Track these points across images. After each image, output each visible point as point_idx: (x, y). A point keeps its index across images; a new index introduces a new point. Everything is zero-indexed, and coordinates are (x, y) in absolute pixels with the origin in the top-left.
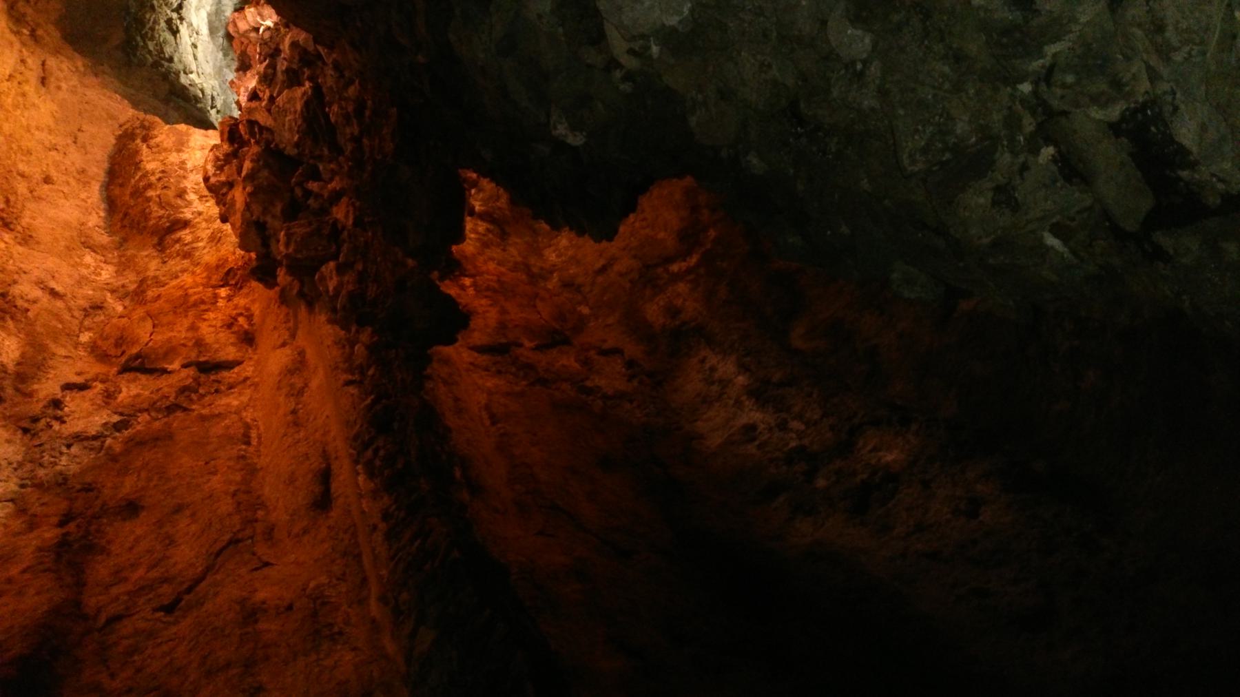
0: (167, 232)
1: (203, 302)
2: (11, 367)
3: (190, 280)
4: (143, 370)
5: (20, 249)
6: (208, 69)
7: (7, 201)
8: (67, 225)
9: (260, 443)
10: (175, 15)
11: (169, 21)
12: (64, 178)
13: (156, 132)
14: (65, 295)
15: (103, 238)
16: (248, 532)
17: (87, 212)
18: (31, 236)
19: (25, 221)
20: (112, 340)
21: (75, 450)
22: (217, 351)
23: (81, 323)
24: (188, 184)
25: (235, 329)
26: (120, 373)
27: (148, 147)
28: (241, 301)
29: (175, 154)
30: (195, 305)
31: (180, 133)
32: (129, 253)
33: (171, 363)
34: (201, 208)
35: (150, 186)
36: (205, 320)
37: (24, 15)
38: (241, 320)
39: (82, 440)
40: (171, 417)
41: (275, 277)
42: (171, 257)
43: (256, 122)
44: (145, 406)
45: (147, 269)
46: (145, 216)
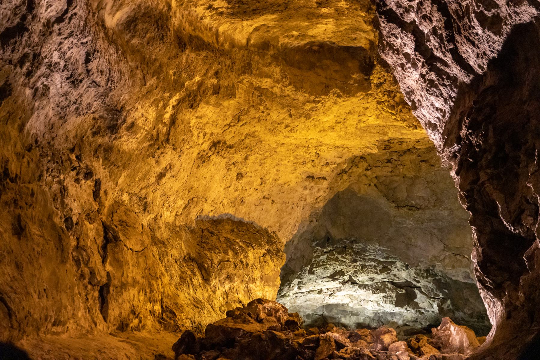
0: (199, 265)
1: (151, 291)
2: (117, 143)
3: (166, 283)
4: (107, 240)
5: (195, 154)
6: (300, 301)
7: (231, 147)
8: (207, 189)
9: (55, 333)
10: (346, 278)
11: (341, 273)
12: (240, 188)
13: (275, 260)
14: (158, 184)
15: (193, 216)
16: (16, 325)
17: (214, 202)
18: (204, 162)
19: (213, 158)
20: (125, 218)
21: (55, 186)
22: (116, 300)
23: (136, 195)
24: (237, 283)
25: (131, 316)
26: (103, 224)
27: (264, 254)
28: (150, 322)
29: (259, 275)
30: (150, 285)
31: (275, 280)
32: (183, 234)
33: (111, 264)
34: (219, 293)
35: (236, 254)
36: (139, 292)
37: (357, 166)
38: (136, 321)
39: (61, 192)
40: (72, 263)
41: (186, 352)
42: (181, 267)
43: (318, 345)
44: (82, 243)
45: (172, 247)
46: (213, 249)
